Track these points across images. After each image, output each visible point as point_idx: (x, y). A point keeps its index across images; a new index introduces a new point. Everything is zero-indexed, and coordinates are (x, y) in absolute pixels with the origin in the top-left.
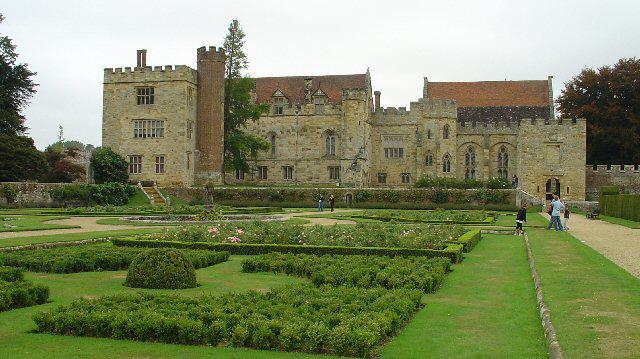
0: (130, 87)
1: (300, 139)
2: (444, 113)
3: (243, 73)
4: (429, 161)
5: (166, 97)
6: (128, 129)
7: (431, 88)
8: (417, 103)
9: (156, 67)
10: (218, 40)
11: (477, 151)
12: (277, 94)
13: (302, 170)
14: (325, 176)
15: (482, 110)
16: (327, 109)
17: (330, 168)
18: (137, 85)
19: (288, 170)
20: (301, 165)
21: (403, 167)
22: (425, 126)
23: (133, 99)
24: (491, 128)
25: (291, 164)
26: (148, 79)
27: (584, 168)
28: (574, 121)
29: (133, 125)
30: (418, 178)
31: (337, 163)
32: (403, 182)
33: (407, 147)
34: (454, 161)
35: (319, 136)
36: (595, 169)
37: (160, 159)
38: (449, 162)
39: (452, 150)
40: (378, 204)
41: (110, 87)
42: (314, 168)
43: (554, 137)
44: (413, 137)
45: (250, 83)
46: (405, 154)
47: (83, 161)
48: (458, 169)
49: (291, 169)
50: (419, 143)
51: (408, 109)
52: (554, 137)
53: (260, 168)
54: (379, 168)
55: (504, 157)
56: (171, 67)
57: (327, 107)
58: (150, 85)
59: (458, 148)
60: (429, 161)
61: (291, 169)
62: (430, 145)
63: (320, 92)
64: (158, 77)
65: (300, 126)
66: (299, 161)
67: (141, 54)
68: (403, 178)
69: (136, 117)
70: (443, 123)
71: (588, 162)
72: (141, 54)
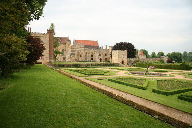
2: (83, 47)
3: (54, 36)
4: (80, 56)
9: (41, 33)
10: (49, 28)
11: (87, 54)
14: (62, 60)
16: (63, 45)
17: (63, 58)
24: (90, 50)
30: (79, 60)
31: (65, 57)
33: (76, 53)
40: (67, 67)
44: (77, 51)
45: (56, 38)
46: (75, 55)
50: (79, 52)
55: (92, 56)
56: (45, 33)
60: (80, 56)
62: (81, 53)
63: (61, 41)
64: (42, 36)
71: (128, 58)
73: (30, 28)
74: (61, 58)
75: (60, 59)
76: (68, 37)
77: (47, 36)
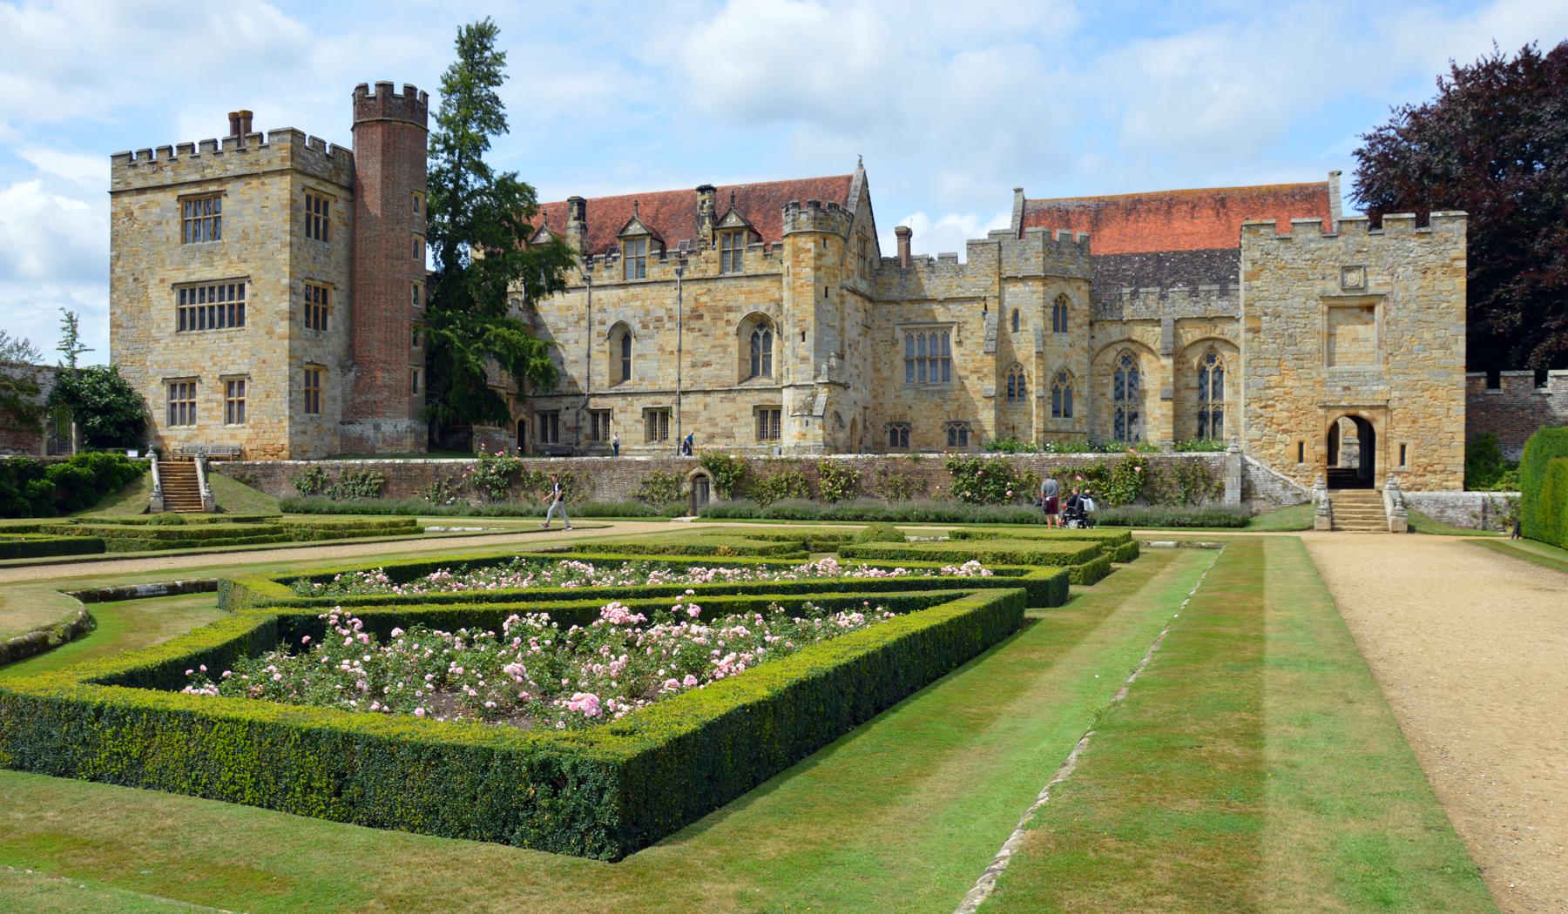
0: (169, 198)
1: (688, 338)
5: (249, 218)
6: (165, 306)
7: (1027, 215)
8: (984, 243)
12: (635, 229)
13: (693, 417)
14: (746, 431)
15: (1159, 259)
18: (183, 191)
19: (657, 419)
20: (688, 403)
21: (950, 407)
22: (1010, 302)
23: (174, 228)
25: (666, 401)
26: (209, 174)
27: (1460, 378)
28: (1422, 221)
29: (175, 297)
32: (951, 443)
34: (1082, 388)
35: (732, 329)
36: (1493, 383)
37: (234, 384)
38: (1069, 392)
39: (1078, 362)
41: (126, 199)
42: (719, 407)
43: (1353, 278)
47: (47, 388)
48: (1094, 413)
49: (665, 414)
51: (963, 260)
52: (1353, 278)
53: (595, 414)
54: (891, 409)
57: (751, 255)
58: (213, 188)
59: (1094, 355)
61: (665, 414)
65: (687, 309)
66: (684, 393)
67: (241, 121)
68: (952, 432)
69: (182, 277)
70: (1055, 290)
71: (1474, 361)
72: (241, 121)
73: (248, 116)
74: (729, 407)
75: (723, 423)
76: (850, 169)
77: (276, 165)
